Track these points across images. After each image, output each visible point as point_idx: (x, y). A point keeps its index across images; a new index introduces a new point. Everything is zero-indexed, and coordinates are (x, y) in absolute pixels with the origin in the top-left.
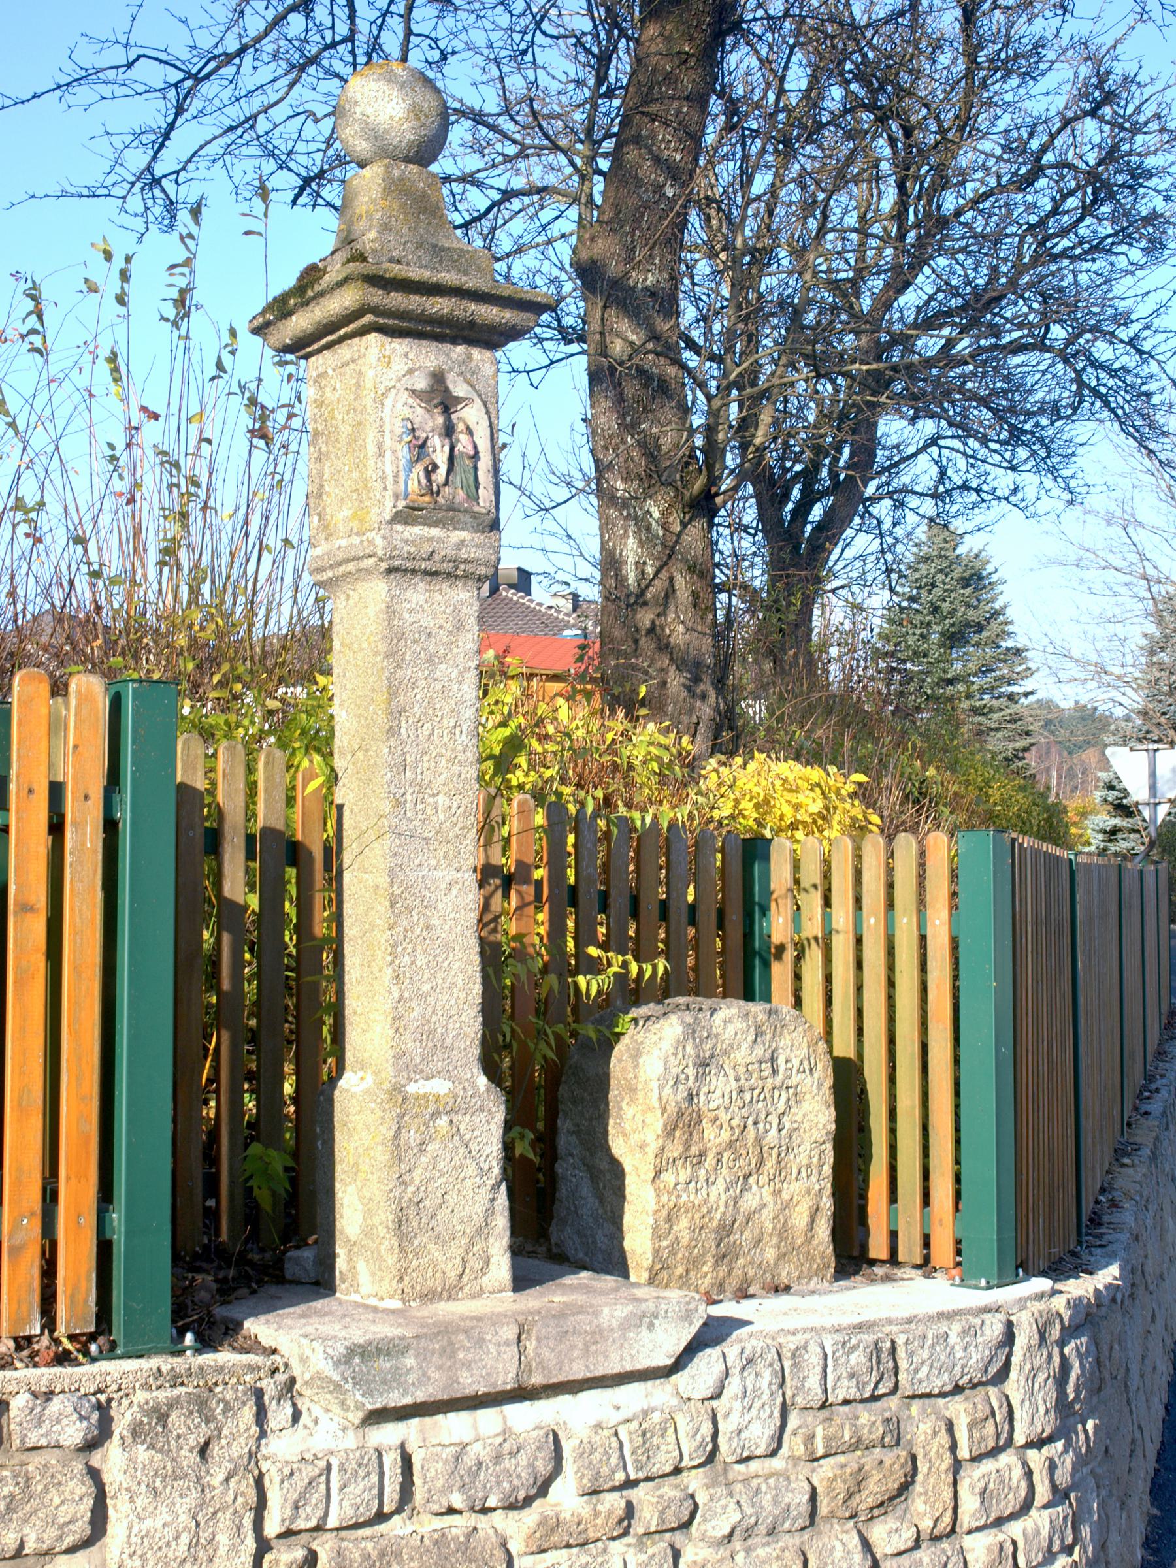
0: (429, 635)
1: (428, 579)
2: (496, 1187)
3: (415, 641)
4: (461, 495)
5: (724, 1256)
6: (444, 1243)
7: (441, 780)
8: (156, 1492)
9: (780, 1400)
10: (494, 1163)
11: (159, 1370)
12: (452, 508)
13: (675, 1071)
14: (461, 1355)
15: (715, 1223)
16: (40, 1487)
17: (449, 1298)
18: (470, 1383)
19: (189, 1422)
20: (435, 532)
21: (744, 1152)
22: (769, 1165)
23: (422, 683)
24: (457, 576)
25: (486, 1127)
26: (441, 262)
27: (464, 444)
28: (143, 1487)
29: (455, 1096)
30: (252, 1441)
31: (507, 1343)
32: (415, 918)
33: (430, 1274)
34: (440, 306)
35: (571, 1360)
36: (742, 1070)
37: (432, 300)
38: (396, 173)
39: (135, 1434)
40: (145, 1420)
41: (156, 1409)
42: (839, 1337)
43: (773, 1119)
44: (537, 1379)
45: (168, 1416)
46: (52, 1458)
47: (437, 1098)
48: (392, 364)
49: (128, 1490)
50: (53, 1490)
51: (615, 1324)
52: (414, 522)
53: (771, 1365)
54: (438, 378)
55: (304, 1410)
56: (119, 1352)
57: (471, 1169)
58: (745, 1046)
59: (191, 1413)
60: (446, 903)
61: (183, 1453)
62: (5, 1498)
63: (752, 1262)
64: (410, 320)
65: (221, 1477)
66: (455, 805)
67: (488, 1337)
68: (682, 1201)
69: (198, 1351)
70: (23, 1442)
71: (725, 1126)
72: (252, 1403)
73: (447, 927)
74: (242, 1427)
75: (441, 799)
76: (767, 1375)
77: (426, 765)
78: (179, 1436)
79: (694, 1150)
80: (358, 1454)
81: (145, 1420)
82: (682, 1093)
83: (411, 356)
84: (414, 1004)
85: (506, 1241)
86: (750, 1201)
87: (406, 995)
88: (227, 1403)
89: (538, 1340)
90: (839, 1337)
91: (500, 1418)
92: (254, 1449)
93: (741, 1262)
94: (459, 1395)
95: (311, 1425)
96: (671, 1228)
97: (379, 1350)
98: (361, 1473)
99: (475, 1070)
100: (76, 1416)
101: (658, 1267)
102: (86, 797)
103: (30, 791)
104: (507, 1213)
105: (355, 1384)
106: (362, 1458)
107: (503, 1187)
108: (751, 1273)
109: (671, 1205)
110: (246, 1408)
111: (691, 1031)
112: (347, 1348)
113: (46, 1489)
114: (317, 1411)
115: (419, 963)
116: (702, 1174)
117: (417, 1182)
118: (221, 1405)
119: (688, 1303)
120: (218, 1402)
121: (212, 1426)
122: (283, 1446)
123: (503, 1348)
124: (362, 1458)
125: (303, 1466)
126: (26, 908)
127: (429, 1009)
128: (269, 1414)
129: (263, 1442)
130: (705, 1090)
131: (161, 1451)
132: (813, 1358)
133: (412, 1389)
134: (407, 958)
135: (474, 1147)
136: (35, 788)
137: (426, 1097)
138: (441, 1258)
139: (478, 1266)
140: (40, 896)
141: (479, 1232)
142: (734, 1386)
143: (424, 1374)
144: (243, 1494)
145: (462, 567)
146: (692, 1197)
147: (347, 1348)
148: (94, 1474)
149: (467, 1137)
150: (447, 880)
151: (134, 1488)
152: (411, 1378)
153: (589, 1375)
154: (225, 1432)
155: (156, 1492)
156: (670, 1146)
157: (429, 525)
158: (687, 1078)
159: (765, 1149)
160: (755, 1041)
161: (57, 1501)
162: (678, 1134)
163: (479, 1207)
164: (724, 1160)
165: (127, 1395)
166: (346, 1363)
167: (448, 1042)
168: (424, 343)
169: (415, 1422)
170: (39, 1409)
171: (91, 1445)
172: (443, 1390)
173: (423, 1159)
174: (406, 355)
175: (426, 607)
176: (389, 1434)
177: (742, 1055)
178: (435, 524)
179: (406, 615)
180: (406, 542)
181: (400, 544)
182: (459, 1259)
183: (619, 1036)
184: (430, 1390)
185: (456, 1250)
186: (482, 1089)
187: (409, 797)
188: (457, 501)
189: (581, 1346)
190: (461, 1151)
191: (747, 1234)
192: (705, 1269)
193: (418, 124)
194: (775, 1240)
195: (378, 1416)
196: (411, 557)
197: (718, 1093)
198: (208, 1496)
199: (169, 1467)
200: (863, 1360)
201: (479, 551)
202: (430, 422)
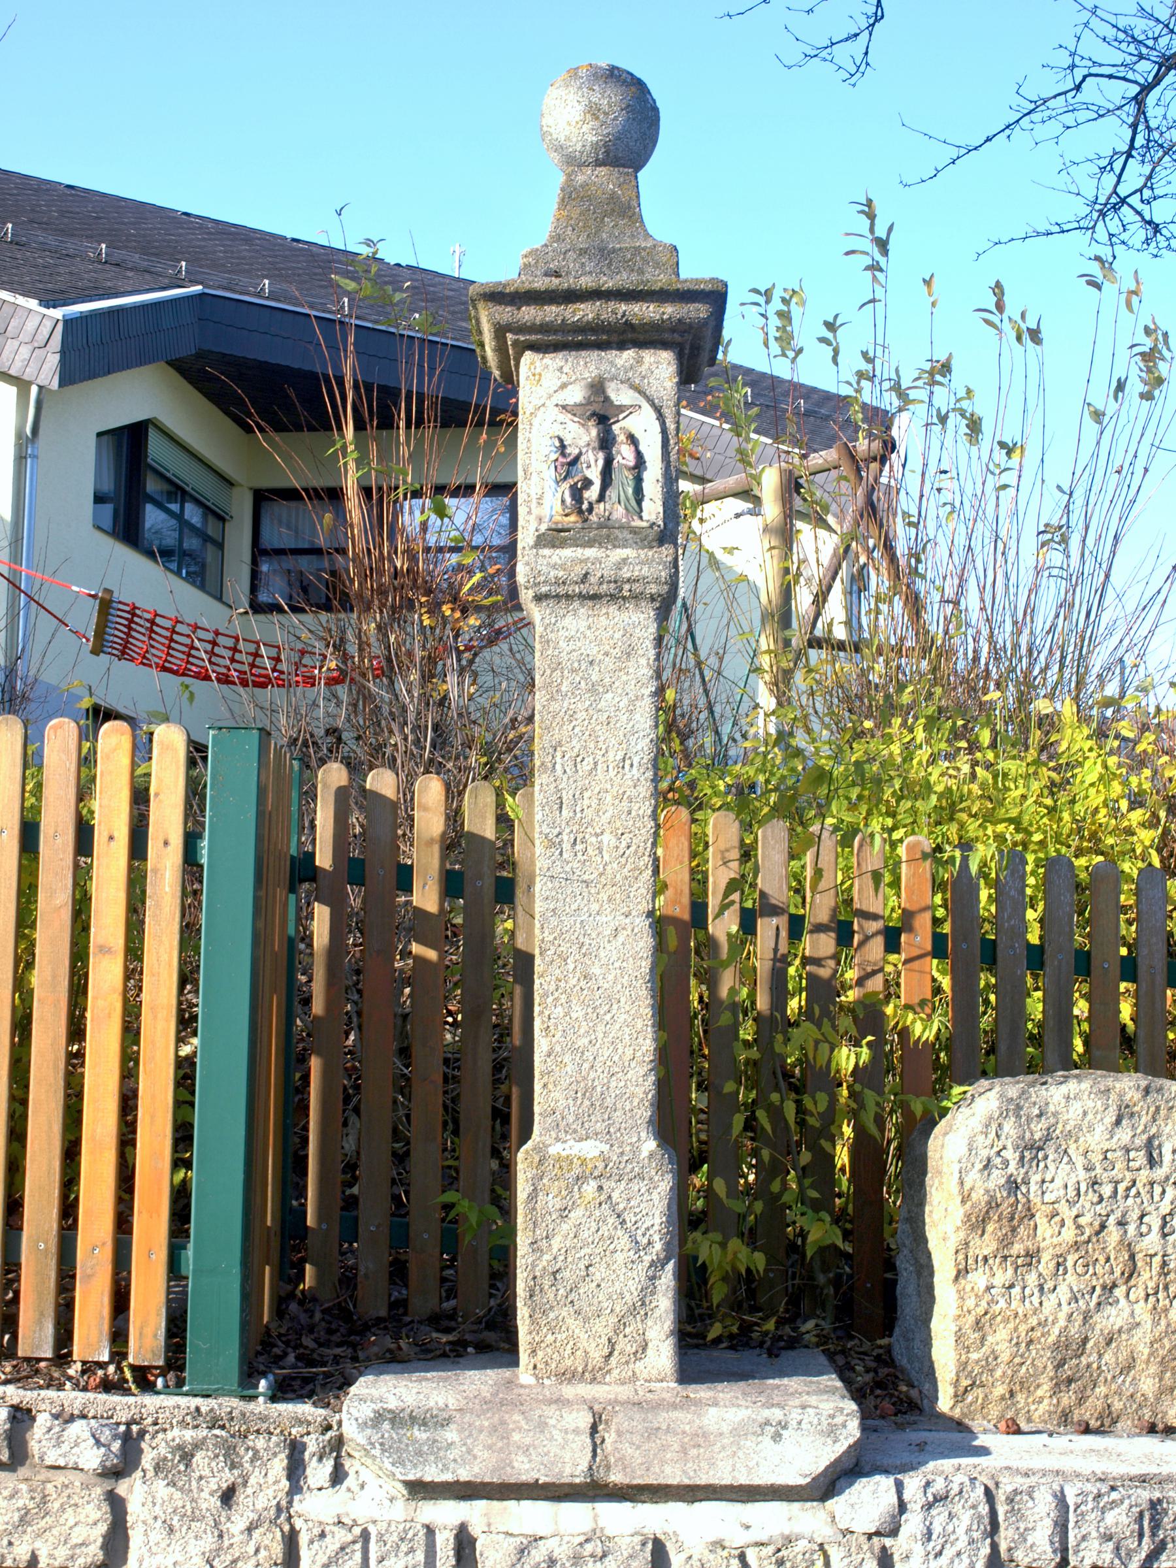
0: (591, 663)
1: (590, 603)
2: (658, 1265)
3: (573, 671)
4: (619, 513)
5: (1070, 1381)
6: (586, 1320)
7: (605, 818)
8: (171, 1530)
9: (986, 1550)
10: (656, 1237)
11: (198, 1409)
12: (607, 524)
13: (985, 1153)
14: (516, 1437)
15: (1052, 1339)
16: (57, 1505)
17: (594, 1380)
18: (525, 1470)
19: (214, 1464)
20: (591, 552)
21: (1102, 1259)
22: (1146, 1275)
23: (581, 715)
24: (624, 598)
25: (646, 1197)
26: (610, 264)
27: (625, 455)
28: (159, 1522)
29: (606, 1161)
30: (281, 1495)
31: (576, 1431)
32: (571, 966)
33: (568, 1351)
34: (585, 312)
35: (663, 1462)
36: (1096, 1158)
37: (571, 307)
38: (580, 179)
39: (157, 1468)
40: (170, 1456)
41: (180, 1447)
42: (1091, 1488)
43: (1154, 1221)
44: (616, 1477)
45: (193, 1456)
46: (76, 1479)
47: (583, 1162)
48: (543, 381)
49: (144, 1522)
50: (70, 1511)
51: (725, 1428)
52: (563, 544)
53: (974, 1507)
54: (598, 388)
55: (352, 1472)
56: (186, 1388)
57: (624, 1242)
58: (1099, 1129)
59: (217, 1456)
60: (610, 951)
61: (203, 1495)
62: (19, 1509)
63: (1118, 1393)
64: (556, 332)
65: (242, 1524)
66: (624, 844)
67: (552, 1422)
68: (996, 1308)
69: (274, 1399)
70: (42, 1459)
71: (1069, 1223)
72: (283, 1456)
73: (611, 977)
74: (271, 1478)
75: (606, 838)
76: (965, 1518)
77: (586, 802)
78: (201, 1478)
79: (1017, 1248)
80: (401, 1527)
81: (170, 1456)
82: (998, 1178)
83: (565, 370)
84: (567, 1058)
85: (668, 1324)
86: (1113, 1317)
87: (558, 1048)
88: (256, 1452)
89: (619, 1434)
90: (1091, 1488)
91: (591, 1514)
92: (284, 1503)
93: (1101, 1390)
94: (512, 1481)
95: (356, 1489)
96: (983, 1339)
97: (413, 1419)
98: (404, 1547)
99: (643, 1135)
100: (92, 1441)
101: (965, 1383)
102: (166, 843)
103: (111, 838)
104: (671, 1294)
105: (383, 1451)
106: (405, 1531)
107: (670, 1266)
108: (1117, 1405)
109: (980, 1310)
110: (276, 1460)
111: (1014, 1108)
112: (375, 1412)
113: (63, 1509)
114: (365, 1475)
115: (574, 1015)
116: (1032, 1279)
117: (555, 1251)
118: (250, 1453)
119: (832, 1417)
120: (247, 1449)
121: (236, 1472)
122: (317, 1505)
123: (571, 1437)
124: (405, 1531)
125: (335, 1529)
126: (105, 950)
127: (586, 1066)
128: (308, 1471)
129: (297, 1498)
130: (1035, 1178)
131: (181, 1489)
132: (1042, 1509)
133: (452, 1465)
134: (559, 1009)
135: (629, 1217)
136: (116, 835)
137: (569, 1160)
138: (584, 1336)
139: (630, 1349)
140: (117, 940)
141: (633, 1311)
142: (912, 1523)
143: (469, 1451)
144: (267, 1548)
145: (627, 587)
146: (1014, 1304)
147: (375, 1412)
148: (117, 1505)
149: (621, 1206)
150: (612, 926)
151: (151, 1521)
152: (453, 1454)
153: (687, 1481)
154: (252, 1481)
155: (171, 1530)
156: (975, 1241)
157: (583, 546)
158: (1006, 1163)
159: (1139, 1256)
160: (1118, 1122)
161: (71, 1523)
162: (990, 1228)
163: (631, 1283)
164: (1070, 1264)
165: (165, 1430)
166: (373, 1427)
167: (609, 1102)
168: (583, 353)
169: (481, 1505)
170: (57, 1429)
171: (117, 1471)
172: (493, 1471)
173: (565, 1227)
174: (560, 369)
175: (588, 633)
176: (446, 1514)
177: (1097, 1139)
178: (590, 544)
179: (563, 644)
180: (554, 567)
181: (545, 569)
182: (604, 1340)
183: (944, 1112)
184: (476, 1470)
185: (603, 1327)
186: (645, 1153)
187: (565, 837)
188: (614, 517)
189: (676, 1447)
190: (611, 1220)
191: (1108, 1357)
192: (1040, 1393)
193: (597, 123)
194: (1153, 1369)
195: (419, 1490)
196: (558, 582)
197: (1059, 1183)
198: (226, 1543)
199: (188, 1507)
200: (1124, 1520)
201: (645, 568)
202: (581, 436)
